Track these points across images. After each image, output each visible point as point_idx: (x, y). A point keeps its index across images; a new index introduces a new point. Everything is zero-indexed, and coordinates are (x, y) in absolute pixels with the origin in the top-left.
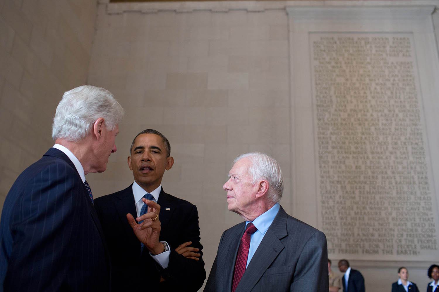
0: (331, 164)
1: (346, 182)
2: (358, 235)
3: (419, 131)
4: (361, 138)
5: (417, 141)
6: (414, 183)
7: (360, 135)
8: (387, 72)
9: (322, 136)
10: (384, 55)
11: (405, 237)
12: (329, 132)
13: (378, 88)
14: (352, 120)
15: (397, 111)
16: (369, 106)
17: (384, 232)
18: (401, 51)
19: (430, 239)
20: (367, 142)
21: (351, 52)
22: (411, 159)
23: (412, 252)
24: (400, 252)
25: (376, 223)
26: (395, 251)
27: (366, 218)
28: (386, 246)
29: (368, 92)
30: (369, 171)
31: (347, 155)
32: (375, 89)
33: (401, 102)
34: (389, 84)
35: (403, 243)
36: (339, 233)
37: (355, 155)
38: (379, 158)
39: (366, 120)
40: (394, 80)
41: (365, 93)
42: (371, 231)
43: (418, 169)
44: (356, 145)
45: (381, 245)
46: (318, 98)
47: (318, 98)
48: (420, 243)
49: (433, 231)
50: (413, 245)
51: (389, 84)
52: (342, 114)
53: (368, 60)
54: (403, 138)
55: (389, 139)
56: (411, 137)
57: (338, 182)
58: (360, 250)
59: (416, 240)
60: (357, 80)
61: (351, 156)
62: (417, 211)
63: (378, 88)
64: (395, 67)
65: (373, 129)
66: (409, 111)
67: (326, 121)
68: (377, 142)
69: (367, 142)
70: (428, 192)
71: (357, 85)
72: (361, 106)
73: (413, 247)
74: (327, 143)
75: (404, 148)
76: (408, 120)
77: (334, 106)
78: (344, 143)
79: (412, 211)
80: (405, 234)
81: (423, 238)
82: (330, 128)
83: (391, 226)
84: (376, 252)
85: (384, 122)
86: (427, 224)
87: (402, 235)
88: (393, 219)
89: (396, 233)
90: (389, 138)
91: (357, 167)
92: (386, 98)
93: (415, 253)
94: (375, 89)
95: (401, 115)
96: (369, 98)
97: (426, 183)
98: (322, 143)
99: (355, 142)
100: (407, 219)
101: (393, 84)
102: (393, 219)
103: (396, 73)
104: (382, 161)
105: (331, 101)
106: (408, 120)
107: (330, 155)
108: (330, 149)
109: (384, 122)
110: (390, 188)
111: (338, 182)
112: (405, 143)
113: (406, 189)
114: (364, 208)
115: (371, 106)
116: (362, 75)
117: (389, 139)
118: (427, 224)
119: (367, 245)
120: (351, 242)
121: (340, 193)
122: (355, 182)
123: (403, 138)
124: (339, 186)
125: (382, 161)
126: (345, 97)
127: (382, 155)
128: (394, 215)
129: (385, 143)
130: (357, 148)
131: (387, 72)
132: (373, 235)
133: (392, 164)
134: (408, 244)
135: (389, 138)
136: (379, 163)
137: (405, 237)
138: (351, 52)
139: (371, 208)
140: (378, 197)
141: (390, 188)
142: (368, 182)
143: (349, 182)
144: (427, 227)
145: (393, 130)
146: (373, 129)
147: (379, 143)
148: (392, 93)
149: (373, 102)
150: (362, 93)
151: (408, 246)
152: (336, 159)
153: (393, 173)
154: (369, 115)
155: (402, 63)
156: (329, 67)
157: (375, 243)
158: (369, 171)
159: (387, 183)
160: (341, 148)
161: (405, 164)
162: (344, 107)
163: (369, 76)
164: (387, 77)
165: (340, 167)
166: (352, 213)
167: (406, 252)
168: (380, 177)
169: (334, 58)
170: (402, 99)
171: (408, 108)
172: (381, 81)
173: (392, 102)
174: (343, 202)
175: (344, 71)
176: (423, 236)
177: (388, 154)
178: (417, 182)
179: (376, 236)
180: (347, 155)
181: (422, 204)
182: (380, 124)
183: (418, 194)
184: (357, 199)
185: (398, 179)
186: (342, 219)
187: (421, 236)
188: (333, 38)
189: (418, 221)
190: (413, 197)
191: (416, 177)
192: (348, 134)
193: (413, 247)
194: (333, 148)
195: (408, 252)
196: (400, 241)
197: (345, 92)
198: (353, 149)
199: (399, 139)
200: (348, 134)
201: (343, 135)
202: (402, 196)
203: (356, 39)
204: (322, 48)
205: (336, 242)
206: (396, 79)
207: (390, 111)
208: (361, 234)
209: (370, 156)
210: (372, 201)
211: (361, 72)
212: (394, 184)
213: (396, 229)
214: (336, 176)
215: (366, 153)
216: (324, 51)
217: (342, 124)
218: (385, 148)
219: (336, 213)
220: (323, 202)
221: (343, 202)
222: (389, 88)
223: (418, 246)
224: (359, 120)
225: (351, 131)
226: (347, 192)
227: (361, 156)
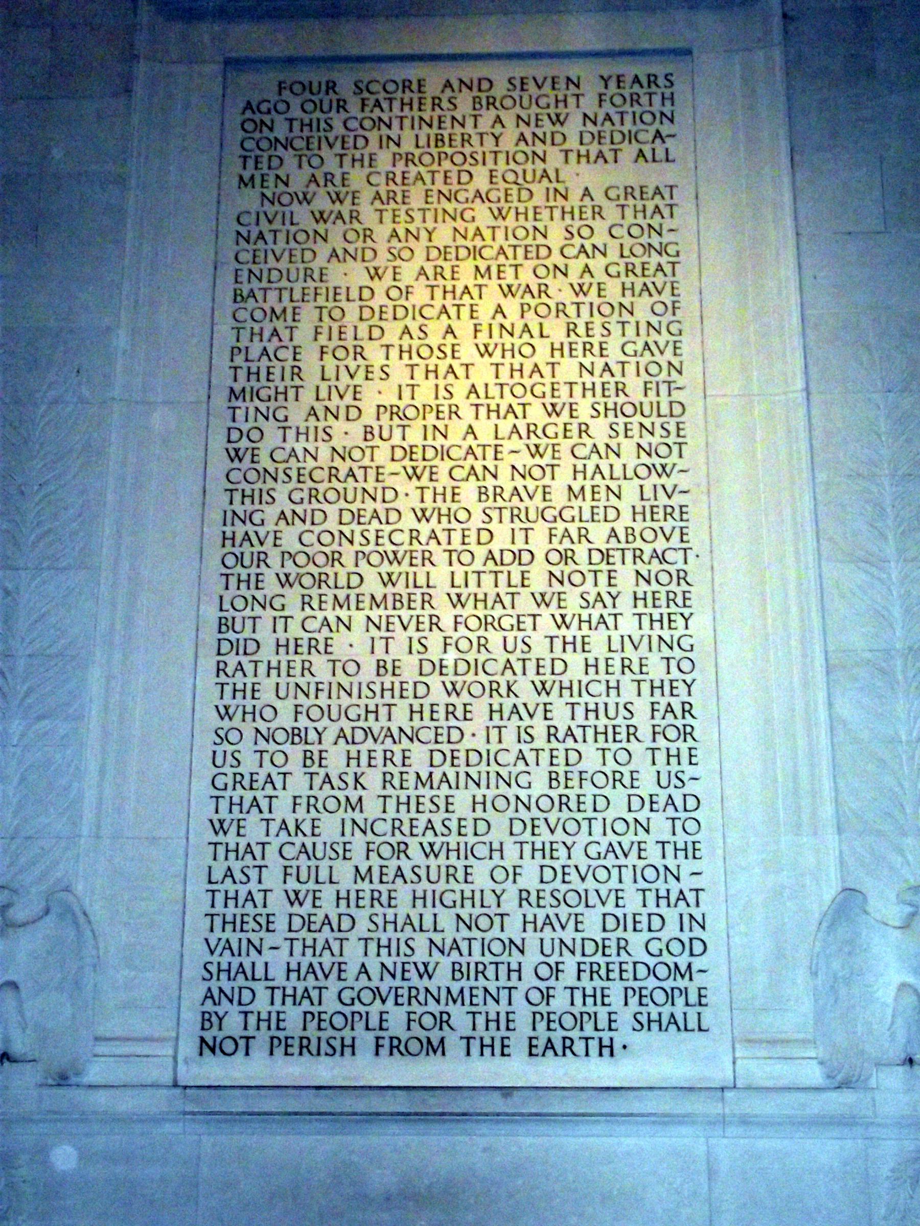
0: (267, 653)
1: (329, 737)
2: (364, 969)
3: (677, 500)
4: (414, 535)
5: (661, 544)
6: (632, 733)
7: (409, 521)
8: (556, 237)
9: (240, 529)
10: (555, 158)
11: (569, 977)
12: (271, 512)
13: (512, 307)
14: (382, 455)
15: (584, 411)
16: (460, 388)
17: (477, 956)
18: (632, 137)
19: (681, 983)
20: (440, 557)
21: (408, 146)
22: (628, 625)
23: (594, 1045)
24: (541, 1043)
25: (446, 919)
26: (518, 1043)
27: (403, 893)
28: (481, 1020)
29: (464, 327)
30: (435, 681)
31: (343, 614)
32: (499, 310)
33: (607, 368)
34: (560, 290)
35: (560, 1002)
36: (278, 961)
37: (374, 614)
38: (485, 623)
39: (445, 453)
40: (587, 269)
41: (450, 331)
42: (421, 955)
43: (656, 670)
44: (385, 568)
45: (459, 1014)
46: (239, 360)
47: (239, 360)
48: (634, 1001)
49: (698, 947)
50: (603, 1012)
51: (560, 290)
52: (338, 427)
53: (481, 182)
54: (599, 534)
55: (539, 541)
56: (638, 526)
57: (295, 735)
58: (366, 1040)
59: (616, 990)
60: (422, 272)
61: (359, 618)
62: (633, 858)
63: (512, 307)
64: (598, 212)
65: (468, 491)
66: (638, 409)
67: (265, 462)
68: (481, 552)
69: (440, 557)
70: (690, 771)
71: (420, 296)
72: (425, 394)
73: (603, 1023)
74: (261, 559)
75: (603, 578)
76: (628, 447)
77: (307, 397)
78: (334, 559)
79: (610, 861)
80: (570, 963)
81: (651, 983)
82: (281, 492)
83: (513, 929)
84: (436, 1048)
85: (524, 460)
86: (671, 915)
87: (556, 970)
88: (523, 897)
89: (532, 957)
90: (540, 531)
91: (380, 666)
92: (542, 356)
93: (607, 1049)
94: (499, 310)
95: (600, 429)
96: (467, 352)
97: (686, 733)
98: (239, 559)
99: (383, 555)
100: (583, 898)
101: (581, 290)
102: (523, 897)
103: (600, 239)
104: (495, 638)
105: (297, 372)
106: (628, 447)
107: (270, 613)
108: (271, 586)
109: (524, 460)
110: (521, 756)
111: (295, 735)
112: (606, 556)
113: (591, 760)
114: (401, 850)
115: (473, 389)
116: (443, 253)
117: (539, 541)
118: (671, 915)
119: (397, 1018)
120: (330, 1004)
121: (298, 784)
122: (368, 732)
123: (599, 534)
124: (296, 753)
125: (495, 638)
126: (359, 353)
127: (498, 611)
128: (529, 879)
129: (517, 556)
130: (389, 580)
131: (556, 237)
132: (426, 972)
133: (540, 648)
134: (578, 1008)
135: (540, 531)
136: (482, 645)
137: (569, 977)
138: (408, 146)
139: (430, 851)
140: (462, 800)
141: (521, 756)
142: (425, 735)
143: (342, 734)
144: (671, 929)
145: (559, 498)
146: (468, 491)
147: (490, 556)
148: (571, 329)
149: (483, 373)
150: (436, 330)
151: (579, 1021)
152: (295, 630)
153: (543, 689)
154: (457, 429)
155: (629, 191)
156: (302, 214)
157: (432, 1006)
158: (435, 681)
159: (509, 736)
160: (319, 582)
161: (598, 648)
162: (348, 399)
163: (476, 253)
164: (556, 258)
165: (307, 668)
166: (344, 872)
167: (568, 1046)
168: (480, 708)
169: (329, 178)
170: (614, 354)
171: (637, 396)
172: (526, 276)
173: (568, 369)
174: (306, 827)
175: (368, 234)
176: (652, 972)
177: (525, 604)
178: (645, 732)
179: (442, 978)
180: (343, 614)
181: (660, 825)
182: (504, 472)
183: (647, 786)
184: (372, 808)
185: (561, 718)
186: (295, 899)
187: (642, 971)
188: (331, 86)
189: (632, 903)
190: (618, 796)
191: (641, 707)
192: (357, 517)
193: (603, 1023)
194: (286, 581)
195: (579, 1047)
196: (547, 997)
197: (363, 332)
198: (373, 586)
199: (584, 535)
200: (357, 517)
201: (332, 524)
202: (572, 794)
203: (432, 88)
204: (281, 132)
205: (262, 1004)
206: (597, 264)
207: (554, 411)
208: (374, 969)
209: (447, 621)
210: (437, 819)
211: (444, 235)
212: (540, 742)
213: (532, 940)
214: (285, 708)
215: (427, 600)
216: (288, 144)
217: (333, 473)
218: (516, 579)
219: (272, 878)
220: (220, 827)
221: (306, 827)
222: (561, 309)
223: (625, 1017)
224: (410, 452)
225: (370, 505)
226: (328, 779)
227: (405, 614)
